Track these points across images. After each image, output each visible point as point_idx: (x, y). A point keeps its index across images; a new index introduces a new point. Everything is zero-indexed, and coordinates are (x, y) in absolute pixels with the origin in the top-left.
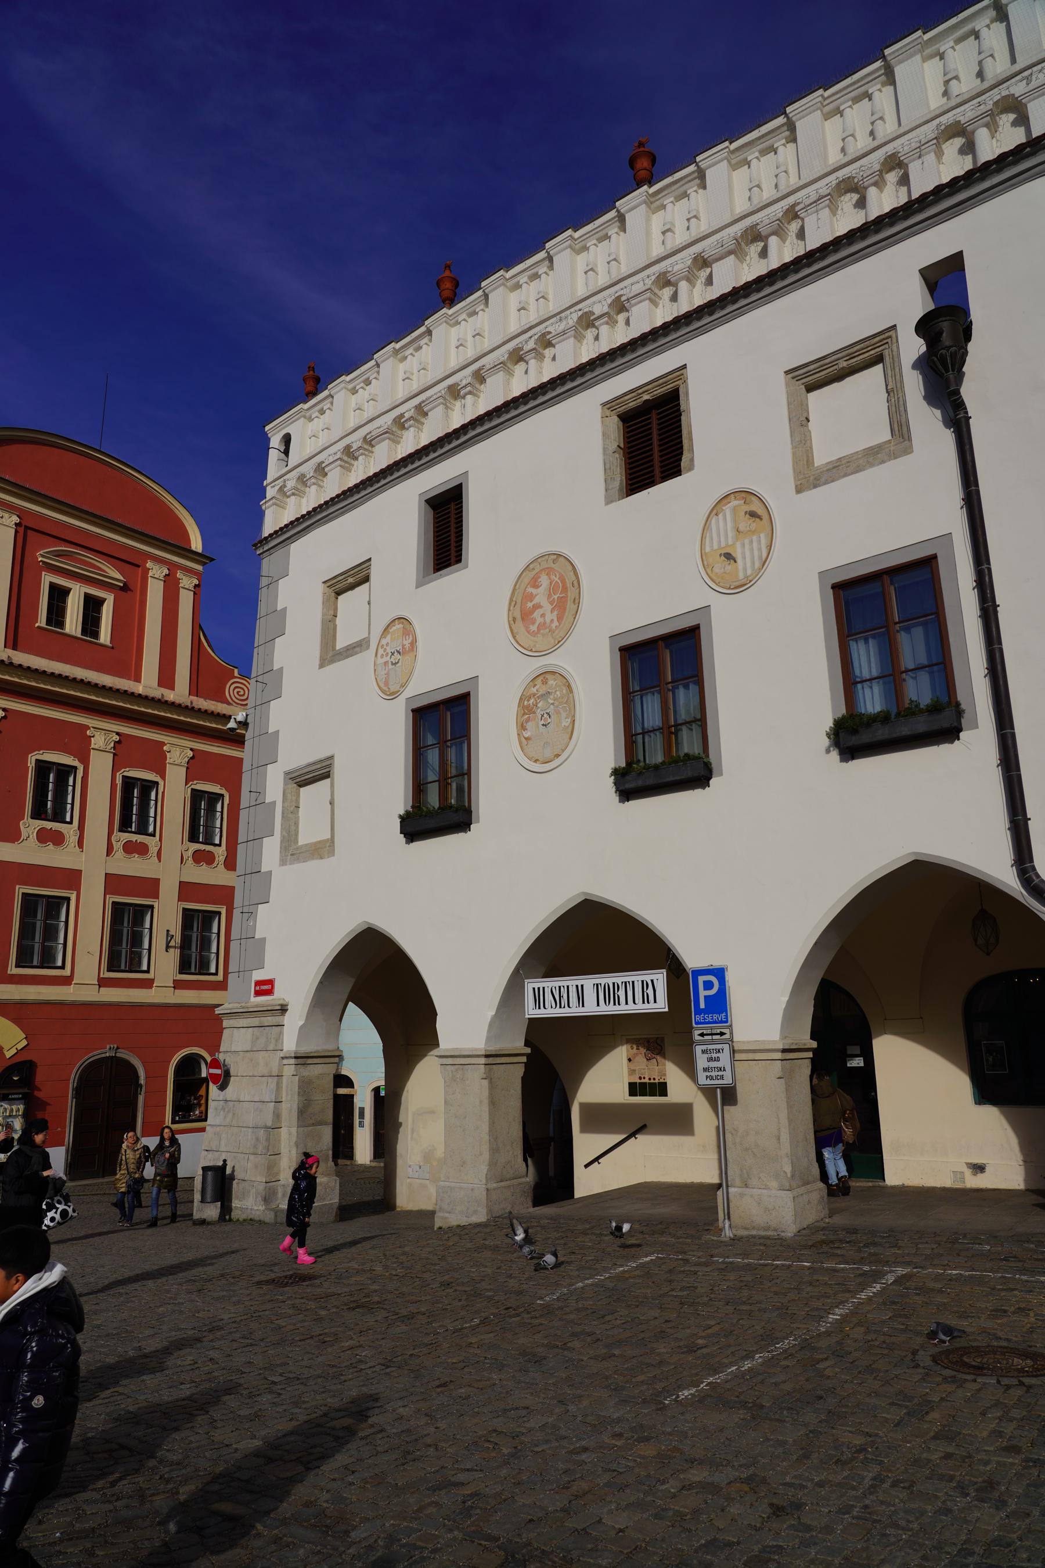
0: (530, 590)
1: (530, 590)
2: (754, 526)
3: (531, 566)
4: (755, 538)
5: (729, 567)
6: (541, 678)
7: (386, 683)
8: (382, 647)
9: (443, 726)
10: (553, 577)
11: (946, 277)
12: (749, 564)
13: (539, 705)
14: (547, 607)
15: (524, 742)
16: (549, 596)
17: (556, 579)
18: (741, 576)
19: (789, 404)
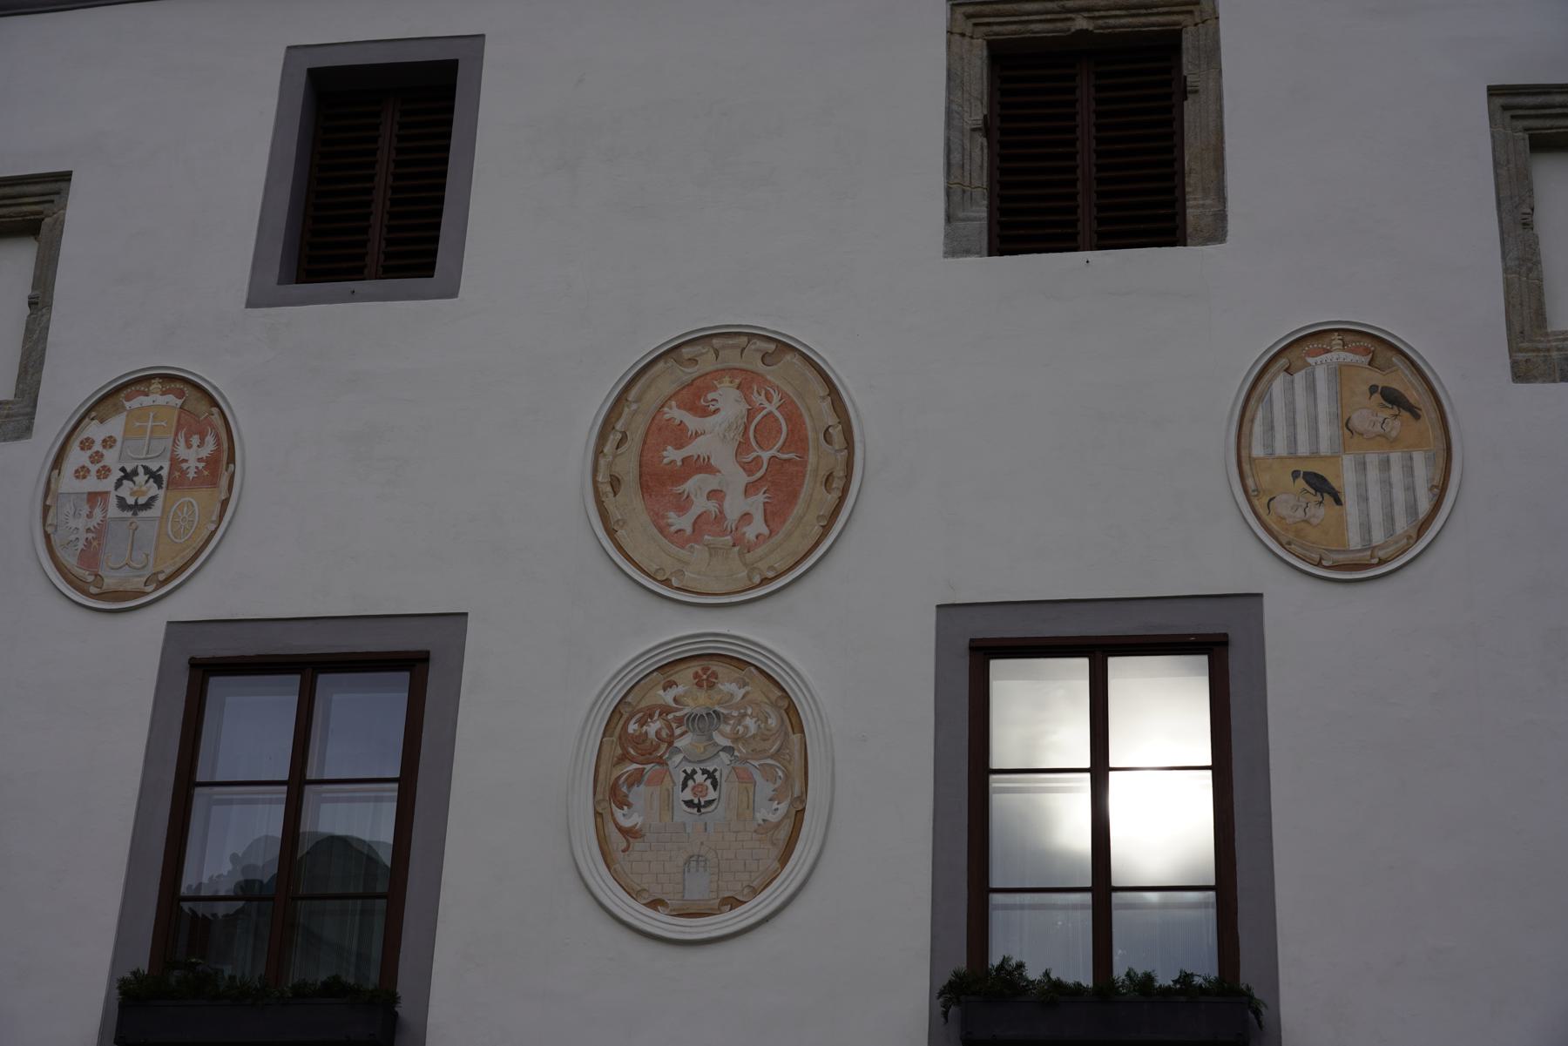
0: (675, 413)
1: (675, 413)
2: (1395, 427)
3: (687, 352)
4: (1396, 457)
5: (1321, 512)
6: (696, 667)
7: (90, 556)
8: (86, 444)
10: (759, 399)
12: (1377, 515)
13: (678, 744)
14: (734, 477)
15: (616, 842)
16: (742, 447)
17: (771, 407)
18: (1354, 540)
19: (1497, 164)
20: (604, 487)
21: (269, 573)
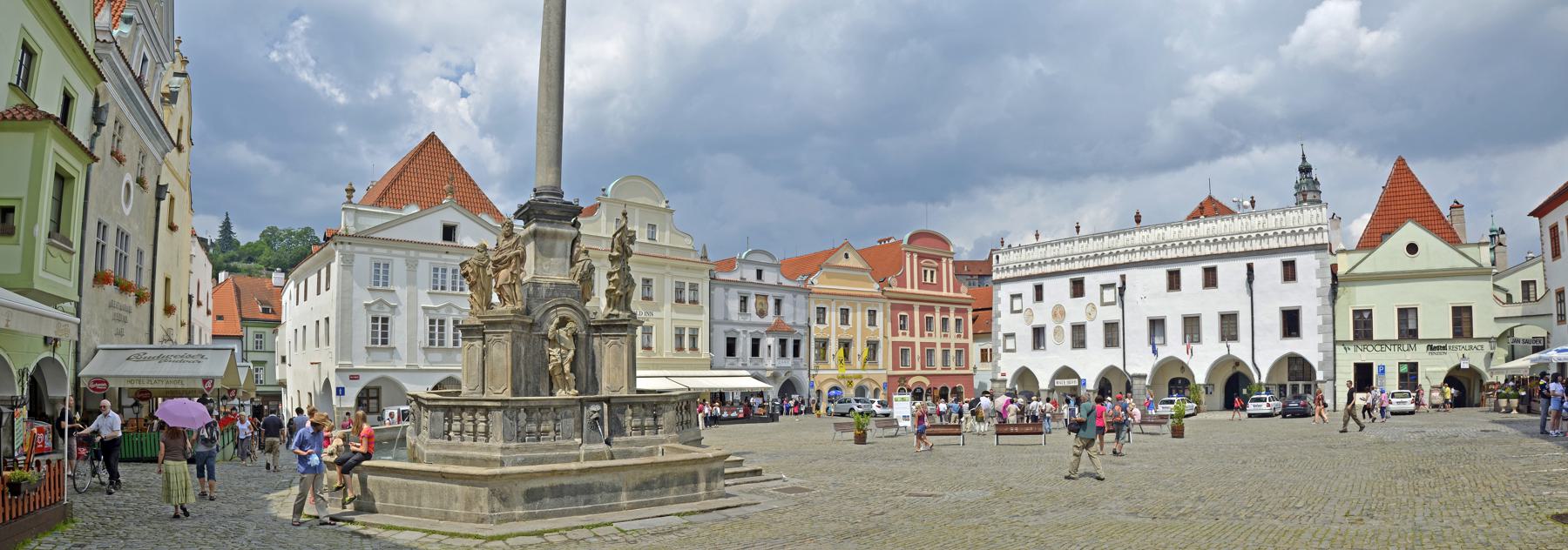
9: (1038, 333)
11: (1123, 277)
21: (1037, 322)
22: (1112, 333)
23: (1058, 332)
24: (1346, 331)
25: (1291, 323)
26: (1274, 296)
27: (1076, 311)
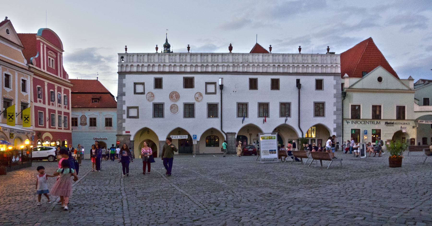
15: (171, 111)
20: (170, 98)
22: (213, 110)
23: (173, 108)
24: (348, 114)
25: (319, 109)
26: (311, 96)
27: (188, 96)
